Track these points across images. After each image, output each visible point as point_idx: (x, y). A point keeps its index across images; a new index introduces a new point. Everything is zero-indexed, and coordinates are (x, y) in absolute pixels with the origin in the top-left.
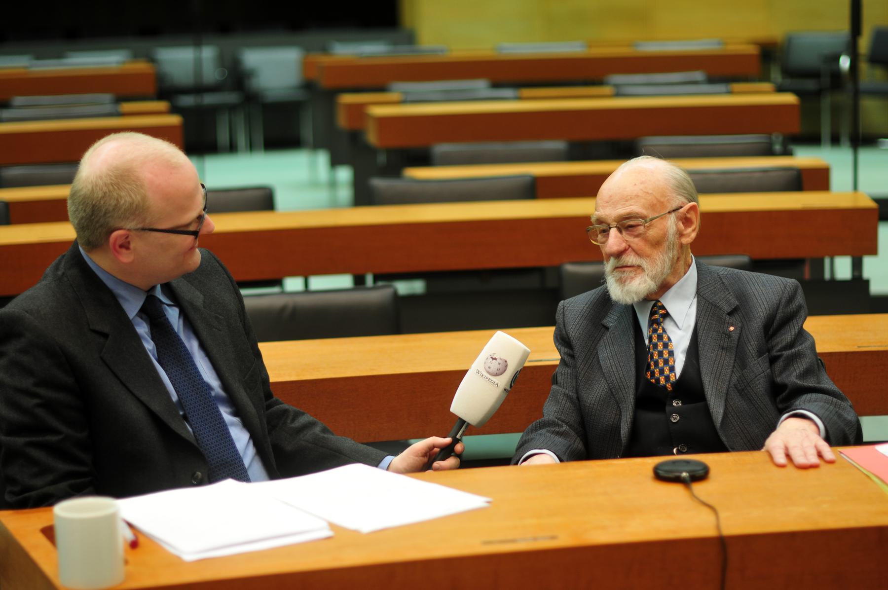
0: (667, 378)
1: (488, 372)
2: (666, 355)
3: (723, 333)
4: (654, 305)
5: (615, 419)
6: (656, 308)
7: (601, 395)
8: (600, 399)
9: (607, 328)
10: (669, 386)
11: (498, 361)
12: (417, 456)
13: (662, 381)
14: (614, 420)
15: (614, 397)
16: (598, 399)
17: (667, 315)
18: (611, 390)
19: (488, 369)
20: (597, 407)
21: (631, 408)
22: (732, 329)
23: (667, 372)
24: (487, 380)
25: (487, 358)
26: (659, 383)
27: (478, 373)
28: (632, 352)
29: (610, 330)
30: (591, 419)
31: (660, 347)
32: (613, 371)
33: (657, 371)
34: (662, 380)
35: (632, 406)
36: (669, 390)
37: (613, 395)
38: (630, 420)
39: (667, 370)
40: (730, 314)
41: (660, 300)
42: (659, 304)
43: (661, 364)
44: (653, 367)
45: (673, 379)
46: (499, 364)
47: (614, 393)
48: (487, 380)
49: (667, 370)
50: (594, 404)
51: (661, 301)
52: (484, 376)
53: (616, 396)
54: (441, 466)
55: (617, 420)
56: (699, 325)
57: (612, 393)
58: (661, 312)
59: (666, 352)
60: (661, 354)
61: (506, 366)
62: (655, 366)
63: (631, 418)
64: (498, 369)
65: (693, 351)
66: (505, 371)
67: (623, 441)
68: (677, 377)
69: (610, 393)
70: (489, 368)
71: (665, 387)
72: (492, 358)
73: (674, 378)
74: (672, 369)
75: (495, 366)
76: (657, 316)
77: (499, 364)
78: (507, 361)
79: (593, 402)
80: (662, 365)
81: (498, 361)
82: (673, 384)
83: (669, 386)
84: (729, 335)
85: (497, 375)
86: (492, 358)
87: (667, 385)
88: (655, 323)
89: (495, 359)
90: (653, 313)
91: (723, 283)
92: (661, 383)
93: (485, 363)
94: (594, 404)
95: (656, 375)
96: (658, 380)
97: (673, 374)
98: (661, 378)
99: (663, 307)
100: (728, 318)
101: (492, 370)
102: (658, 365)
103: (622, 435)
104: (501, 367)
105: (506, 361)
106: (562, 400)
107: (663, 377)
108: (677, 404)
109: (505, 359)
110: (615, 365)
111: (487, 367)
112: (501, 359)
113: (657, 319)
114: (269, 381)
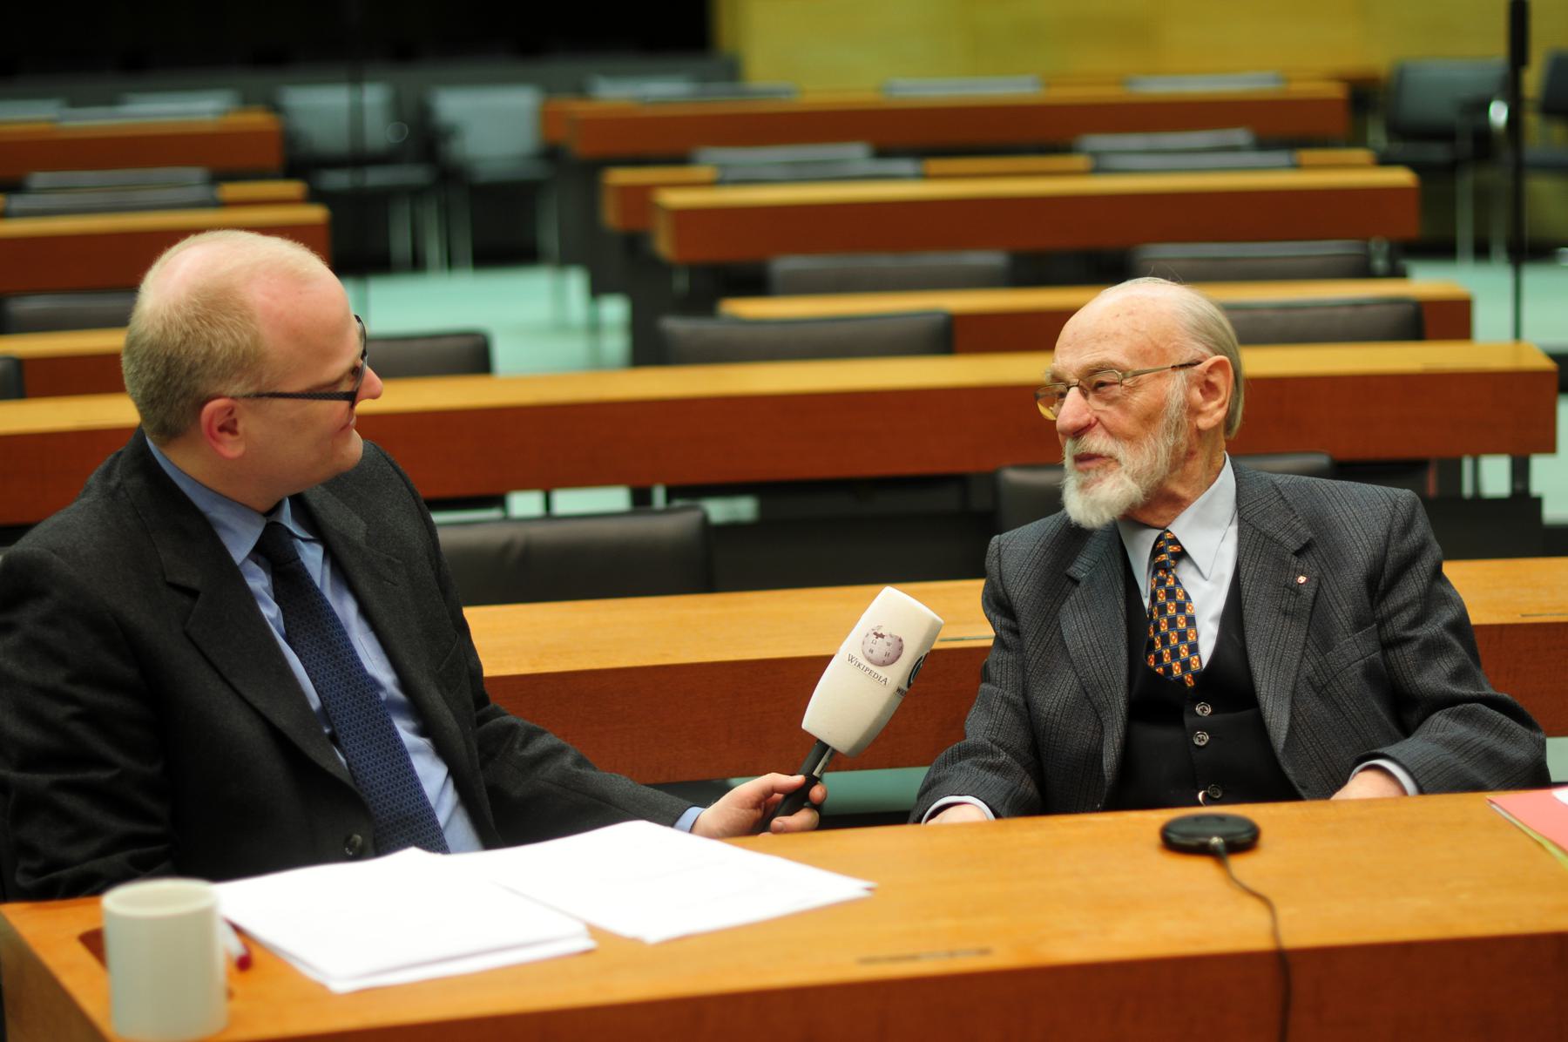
0: (1186, 665)
2: (1182, 624)
3: (1285, 586)
4: (1159, 538)
6: (1162, 543)
9: (1076, 582)
10: (1188, 678)
11: (887, 639)
12: (743, 808)
13: (1177, 670)
15: (1091, 702)
16: (1062, 705)
17: (1182, 555)
18: (1084, 689)
19: (870, 654)
21: (1121, 719)
22: (1302, 579)
23: (1184, 654)
24: (867, 672)
26: (1172, 673)
27: (851, 660)
28: (1122, 622)
29: (1081, 584)
30: (1049, 740)
32: (1088, 656)
33: (1166, 652)
34: (1177, 668)
36: (1189, 685)
37: (1089, 698)
38: (1118, 740)
39: (1184, 651)
40: (1298, 553)
41: (1169, 528)
42: (1168, 536)
43: (1174, 641)
44: (1160, 646)
45: (1195, 666)
46: (889, 644)
47: (1091, 695)
48: (867, 672)
49: (1184, 651)
50: (1055, 715)
51: (1171, 530)
54: (785, 825)
55: (1097, 741)
56: (1243, 571)
57: (1086, 693)
58: (1172, 549)
59: (1181, 620)
60: (1172, 622)
61: (901, 649)
62: (1162, 645)
64: (887, 655)
65: (1234, 616)
66: (898, 657)
67: (1107, 778)
68: (1204, 665)
69: (1085, 695)
70: (871, 651)
71: (1181, 680)
72: (875, 634)
73: (1198, 665)
74: (1194, 649)
75: (881, 648)
76: (1164, 557)
77: (889, 644)
78: (902, 638)
79: (1052, 711)
80: (1176, 641)
81: (887, 639)
82: (1196, 676)
83: (1188, 678)
84: (1297, 590)
85: (885, 663)
86: (875, 634)
87: (1186, 677)
88: (1163, 569)
89: (882, 636)
90: (1156, 552)
91: (1282, 498)
92: (1175, 673)
94: (1055, 715)
95: (1165, 660)
96: (1169, 669)
97: (1196, 657)
98: (1174, 664)
99: (1175, 541)
100: (1294, 560)
101: (875, 656)
102: (1168, 643)
103: (1105, 767)
104: (892, 650)
105: (900, 640)
106: (999, 709)
107: (1178, 663)
108: (1203, 710)
109: (900, 635)
110: (1092, 645)
112: (891, 636)
113: (1165, 561)
114: (482, 674)
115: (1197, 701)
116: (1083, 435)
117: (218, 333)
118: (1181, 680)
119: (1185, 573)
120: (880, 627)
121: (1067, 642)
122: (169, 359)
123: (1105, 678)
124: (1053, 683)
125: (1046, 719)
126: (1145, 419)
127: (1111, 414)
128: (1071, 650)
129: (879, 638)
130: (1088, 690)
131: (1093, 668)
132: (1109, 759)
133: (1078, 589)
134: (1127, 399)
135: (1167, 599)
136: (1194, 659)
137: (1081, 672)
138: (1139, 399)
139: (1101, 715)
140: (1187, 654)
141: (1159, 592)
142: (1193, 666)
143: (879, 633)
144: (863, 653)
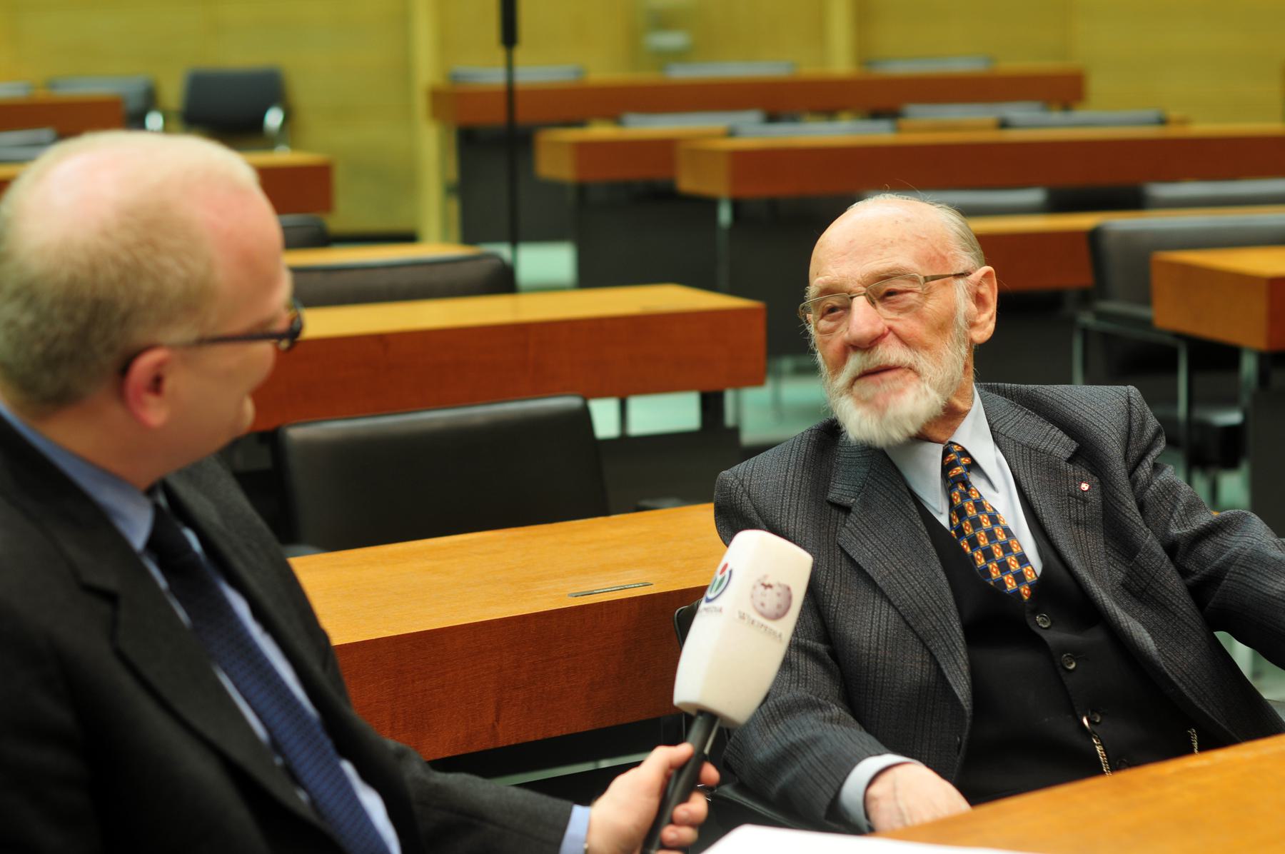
0: (1019, 577)
1: (763, 615)
2: (984, 541)
5: (922, 671)
6: (953, 457)
7: (887, 629)
8: (886, 638)
9: (847, 510)
13: (1011, 584)
14: (921, 674)
15: (914, 632)
16: (882, 638)
19: (761, 608)
20: (885, 654)
21: (962, 645)
23: (1015, 566)
24: (763, 629)
25: (754, 587)
27: (742, 616)
28: (929, 544)
29: (853, 510)
30: (876, 677)
31: (986, 524)
32: (899, 583)
33: (993, 567)
34: (1010, 581)
35: (962, 642)
37: (911, 627)
38: (966, 668)
39: (1013, 563)
41: (953, 440)
42: (956, 448)
43: (999, 554)
44: (983, 561)
46: (779, 595)
47: (912, 624)
49: (1013, 563)
50: (877, 649)
52: (756, 623)
53: (917, 629)
55: (928, 672)
57: (907, 623)
58: (964, 461)
59: (998, 531)
61: (790, 598)
62: (986, 559)
63: (967, 665)
64: (779, 606)
67: (966, 708)
68: (1038, 575)
69: (903, 625)
70: (763, 605)
71: (1017, 593)
72: (763, 585)
73: (1033, 576)
74: (1023, 560)
75: (771, 600)
77: (779, 595)
80: (1001, 554)
81: (776, 589)
85: (777, 617)
86: (763, 585)
87: (1022, 590)
89: (770, 586)
90: (946, 468)
92: (1009, 586)
93: (752, 597)
94: (877, 649)
95: (994, 575)
96: (1001, 583)
98: (1005, 578)
99: (965, 453)
102: (993, 556)
103: (960, 698)
105: (789, 589)
107: (1010, 576)
109: (785, 582)
111: (758, 605)
112: (780, 585)
113: (962, 474)
115: (1036, 612)
116: (877, 345)
117: (168, 262)
118: (1017, 593)
119: (978, 484)
120: (766, 577)
121: (867, 570)
122: (97, 303)
123: (926, 604)
124: (862, 617)
125: (869, 655)
126: (940, 328)
127: (905, 324)
128: (877, 579)
129: (769, 590)
130: (908, 618)
131: (909, 595)
132: (961, 689)
133: (852, 514)
134: (922, 307)
135: (977, 512)
136: (1027, 571)
137: (895, 600)
138: (933, 306)
139: (929, 644)
140: (1017, 566)
141: (967, 505)
142: (1029, 578)
143: (767, 582)
144: (755, 607)
